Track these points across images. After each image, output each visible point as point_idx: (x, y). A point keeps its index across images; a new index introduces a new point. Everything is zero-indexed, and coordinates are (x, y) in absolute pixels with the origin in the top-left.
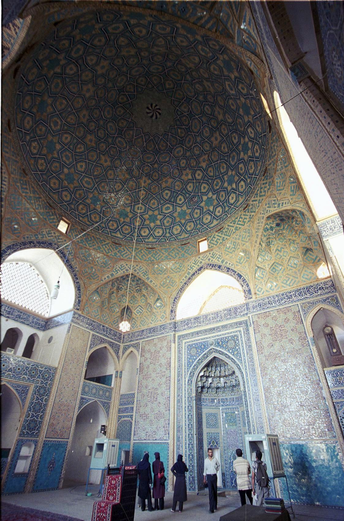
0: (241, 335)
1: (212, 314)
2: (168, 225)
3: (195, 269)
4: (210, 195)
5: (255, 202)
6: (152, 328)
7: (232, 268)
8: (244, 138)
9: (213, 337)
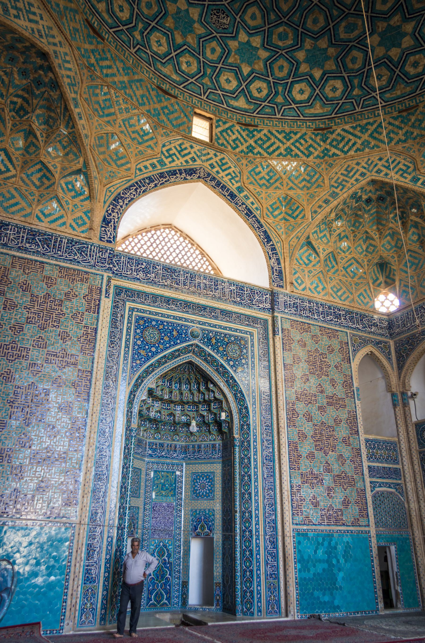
0: (252, 341)
1: (205, 278)
2: (146, 11)
3: (177, 162)
4: (256, 41)
5: (351, 137)
6: (40, 233)
7: (257, 213)
8: (405, 20)
9: (199, 322)
